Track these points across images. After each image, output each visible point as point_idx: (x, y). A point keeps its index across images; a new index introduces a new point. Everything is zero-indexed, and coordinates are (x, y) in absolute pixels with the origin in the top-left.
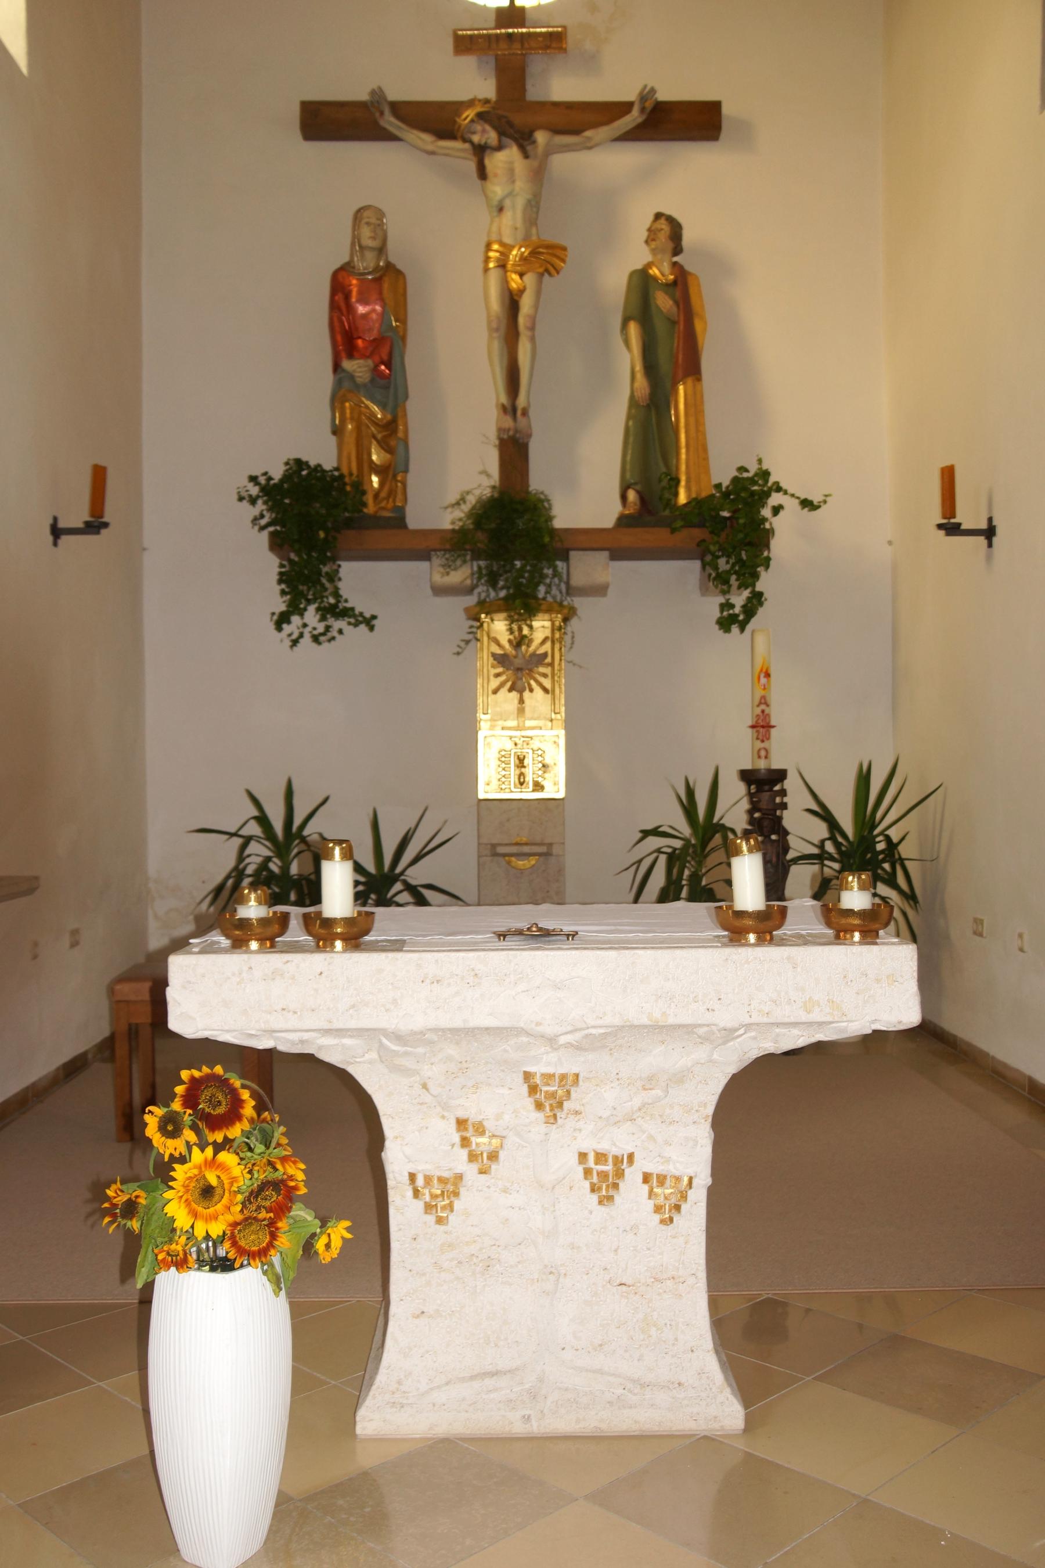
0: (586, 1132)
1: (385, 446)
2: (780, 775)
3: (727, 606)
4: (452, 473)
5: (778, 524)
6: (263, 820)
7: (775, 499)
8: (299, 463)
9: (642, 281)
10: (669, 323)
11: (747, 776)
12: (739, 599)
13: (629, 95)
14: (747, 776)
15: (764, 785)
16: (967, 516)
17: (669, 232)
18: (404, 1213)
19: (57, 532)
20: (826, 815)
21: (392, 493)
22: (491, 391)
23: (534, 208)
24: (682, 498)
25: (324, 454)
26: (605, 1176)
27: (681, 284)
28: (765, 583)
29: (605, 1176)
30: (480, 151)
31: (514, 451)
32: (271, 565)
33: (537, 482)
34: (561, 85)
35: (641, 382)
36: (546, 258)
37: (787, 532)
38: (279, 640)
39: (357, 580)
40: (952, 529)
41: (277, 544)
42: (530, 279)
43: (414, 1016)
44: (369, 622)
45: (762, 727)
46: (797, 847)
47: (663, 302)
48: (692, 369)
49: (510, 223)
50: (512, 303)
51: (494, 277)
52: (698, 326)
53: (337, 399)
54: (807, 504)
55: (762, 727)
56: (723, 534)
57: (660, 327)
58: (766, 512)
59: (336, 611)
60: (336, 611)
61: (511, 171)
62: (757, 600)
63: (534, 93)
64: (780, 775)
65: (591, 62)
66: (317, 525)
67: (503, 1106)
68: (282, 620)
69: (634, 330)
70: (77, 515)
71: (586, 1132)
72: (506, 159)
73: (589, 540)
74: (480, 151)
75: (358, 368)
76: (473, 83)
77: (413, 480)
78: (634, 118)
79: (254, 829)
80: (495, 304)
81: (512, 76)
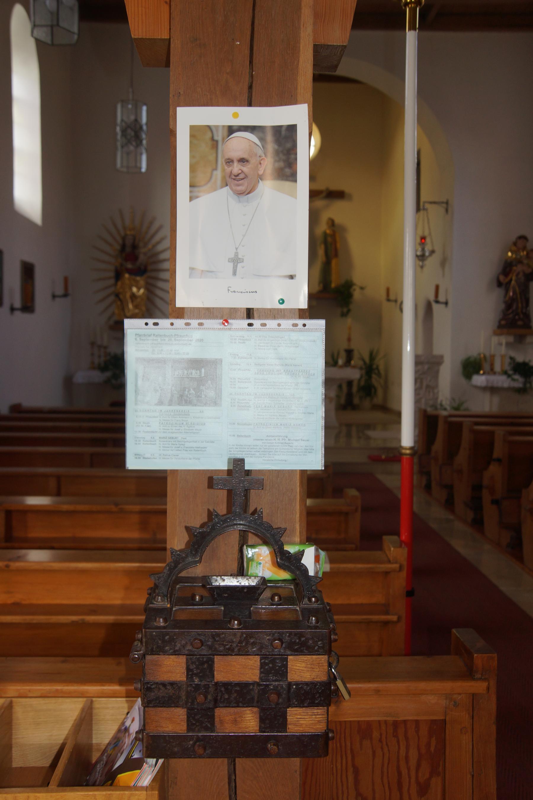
7: (354, 287)
9: (325, 235)
12: (345, 310)
16: (392, 297)
17: (332, 223)
20: (363, 360)
24: (333, 285)
27: (333, 235)
28: (352, 307)
35: (324, 259)
37: (357, 294)
40: (388, 300)
45: (349, 340)
47: (329, 239)
48: (336, 255)
54: (362, 288)
55: (349, 340)
62: (349, 311)
69: (323, 246)
78: (324, 194)
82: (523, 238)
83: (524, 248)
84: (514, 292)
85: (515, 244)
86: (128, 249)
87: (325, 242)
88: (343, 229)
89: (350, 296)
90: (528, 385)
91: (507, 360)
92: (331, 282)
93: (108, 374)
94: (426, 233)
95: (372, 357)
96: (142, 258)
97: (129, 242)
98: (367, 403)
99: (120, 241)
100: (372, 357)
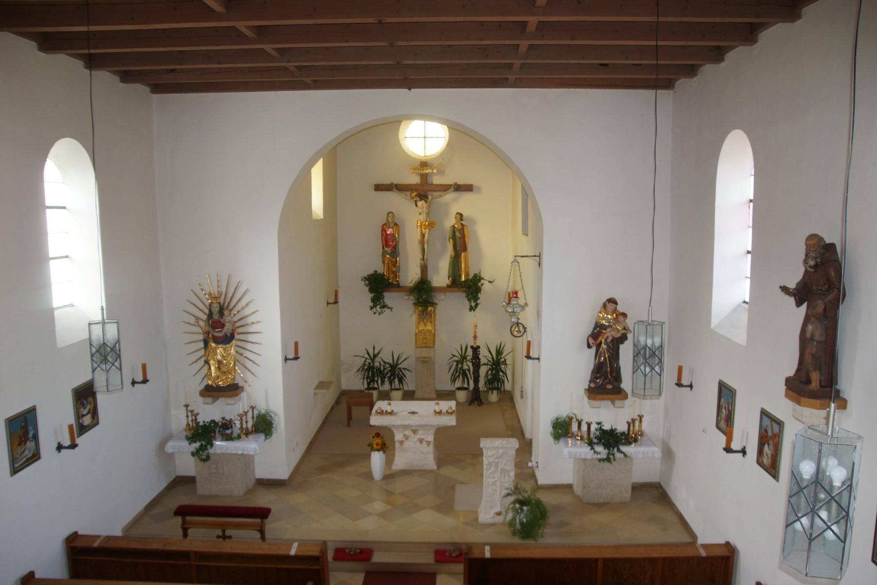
0: (418, 436)
1: (394, 266)
2: (479, 347)
3: (471, 306)
4: (411, 275)
5: (483, 288)
6: (368, 353)
7: (482, 281)
8: (375, 272)
10: (460, 240)
11: (472, 347)
12: (473, 304)
13: (452, 183)
14: (472, 347)
15: (476, 350)
17: (460, 216)
18: (397, 445)
19: (328, 303)
21: (396, 277)
22: (419, 255)
23: (428, 214)
25: (380, 270)
26: (421, 441)
29: (421, 441)
30: (416, 202)
31: (424, 269)
32: (370, 296)
33: (429, 278)
34: (437, 180)
35: (453, 253)
36: (431, 225)
37: (486, 287)
38: (371, 312)
39: (389, 297)
41: (371, 291)
42: (427, 230)
43: (398, 423)
44: (391, 309)
45: (475, 337)
46: (483, 360)
47: (458, 234)
48: (465, 249)
49: (423, 217)
50: (423, 235)
51: (419, 229)
52: (466, 239)
53: (383, 256)
55: (475, 337)
56: (471, 288)
57: (458, 239)
58: (480, 284)
59: (384, 306)
60: (384, 306)
61: (423, 207)
62: (477, 305)
63: (429, 181)
64: (479, 347)
65: (441, 172)
66: (379, 286)
67: (408, 432)
68: (372, 308)
70: (333, 300)
71: (418, 436)
72: (421, 203)
73: (441, 290)
74: (416, 202)
75: (388, 250)
76: (415, 180)
77: (401, 274)
79: (367, 356)
80: (419, 236)
81: (424, 177)
82: (612, 301)
83: (615, 311)
84: (605, 358)
85: (605, 306)
86: (216, 317)
87: (454, 237)
88: (473, 221)
89: (478, 290)
90: (611, 457)
91: (594, 427)
92: (460, 276)
93: (197, 445)
94: (518, 288)
95: (499, 352)
96: (228, 328)
97: (216, 309)
98: (494, 397)
99: (207, 312)
100: (499, 352)
